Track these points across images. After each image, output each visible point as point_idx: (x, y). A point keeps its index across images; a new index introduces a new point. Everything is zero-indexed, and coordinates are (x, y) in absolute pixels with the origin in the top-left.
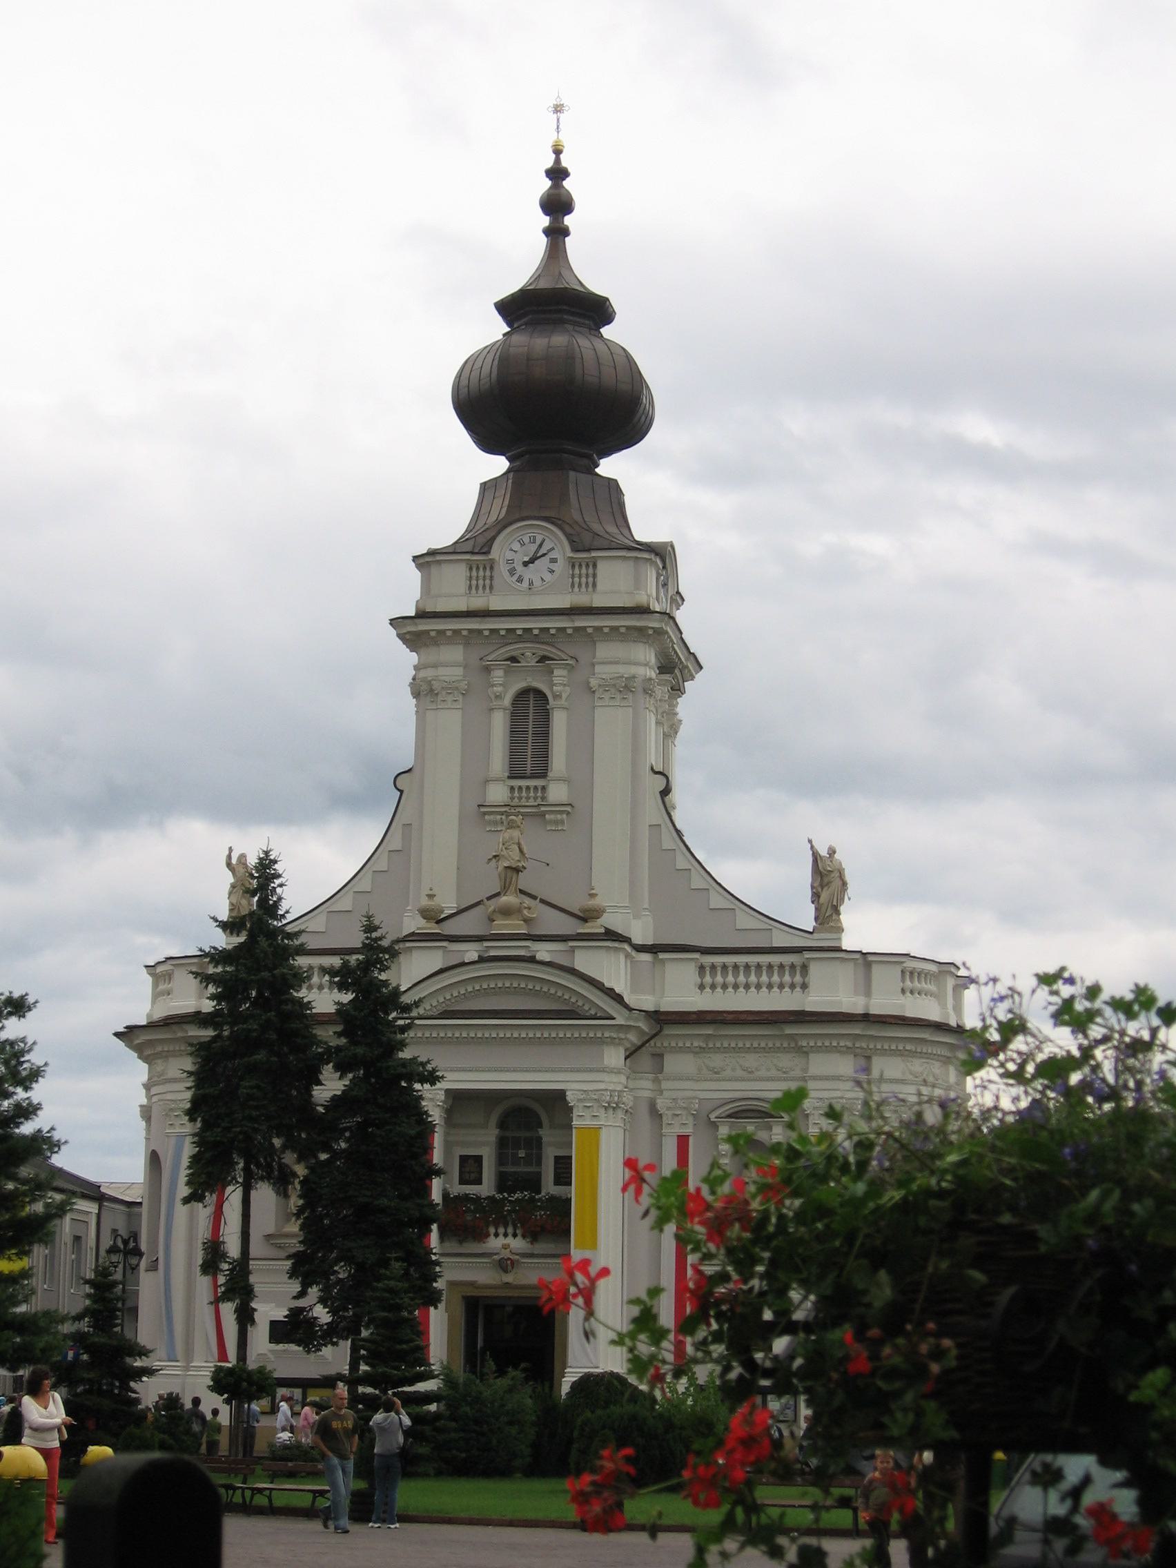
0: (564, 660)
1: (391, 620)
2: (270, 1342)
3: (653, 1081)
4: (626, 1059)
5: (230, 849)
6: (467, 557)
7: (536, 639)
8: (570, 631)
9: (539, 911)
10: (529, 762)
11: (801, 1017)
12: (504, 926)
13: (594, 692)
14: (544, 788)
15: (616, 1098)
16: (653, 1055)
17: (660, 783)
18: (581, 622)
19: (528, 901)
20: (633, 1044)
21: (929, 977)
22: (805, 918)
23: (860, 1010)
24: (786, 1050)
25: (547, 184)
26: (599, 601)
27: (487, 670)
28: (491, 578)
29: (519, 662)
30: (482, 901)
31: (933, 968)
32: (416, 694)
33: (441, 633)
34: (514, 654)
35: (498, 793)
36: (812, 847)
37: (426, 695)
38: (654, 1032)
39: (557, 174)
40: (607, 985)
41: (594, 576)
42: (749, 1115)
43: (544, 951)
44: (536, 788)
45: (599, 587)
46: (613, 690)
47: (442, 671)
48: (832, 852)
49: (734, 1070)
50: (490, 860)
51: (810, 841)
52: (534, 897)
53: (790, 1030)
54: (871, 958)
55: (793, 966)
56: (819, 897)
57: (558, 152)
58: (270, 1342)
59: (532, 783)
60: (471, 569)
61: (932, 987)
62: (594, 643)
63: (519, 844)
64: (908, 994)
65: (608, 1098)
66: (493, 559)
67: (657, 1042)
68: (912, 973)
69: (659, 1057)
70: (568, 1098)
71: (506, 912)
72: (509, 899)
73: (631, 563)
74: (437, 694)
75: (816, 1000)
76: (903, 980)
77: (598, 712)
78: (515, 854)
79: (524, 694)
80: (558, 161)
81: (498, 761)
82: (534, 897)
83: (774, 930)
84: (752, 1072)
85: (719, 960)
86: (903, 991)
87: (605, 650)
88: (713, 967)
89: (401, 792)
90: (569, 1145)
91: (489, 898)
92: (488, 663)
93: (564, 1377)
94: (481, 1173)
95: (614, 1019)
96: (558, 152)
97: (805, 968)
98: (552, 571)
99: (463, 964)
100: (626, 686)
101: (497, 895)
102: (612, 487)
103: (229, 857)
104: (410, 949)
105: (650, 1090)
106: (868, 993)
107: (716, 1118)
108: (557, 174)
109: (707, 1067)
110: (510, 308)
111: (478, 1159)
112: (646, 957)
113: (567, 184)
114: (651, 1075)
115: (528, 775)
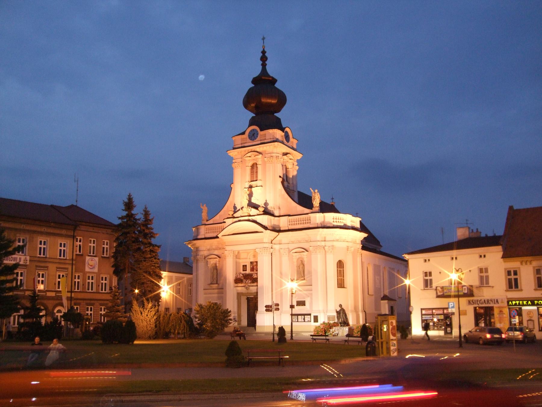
23: (317, 227)
25: (261, 54)
39: (264, 52)
80: (264, 49)
94: (246, 268)
108: (264, 52)
111: (246, 266)
115: (255, 180)
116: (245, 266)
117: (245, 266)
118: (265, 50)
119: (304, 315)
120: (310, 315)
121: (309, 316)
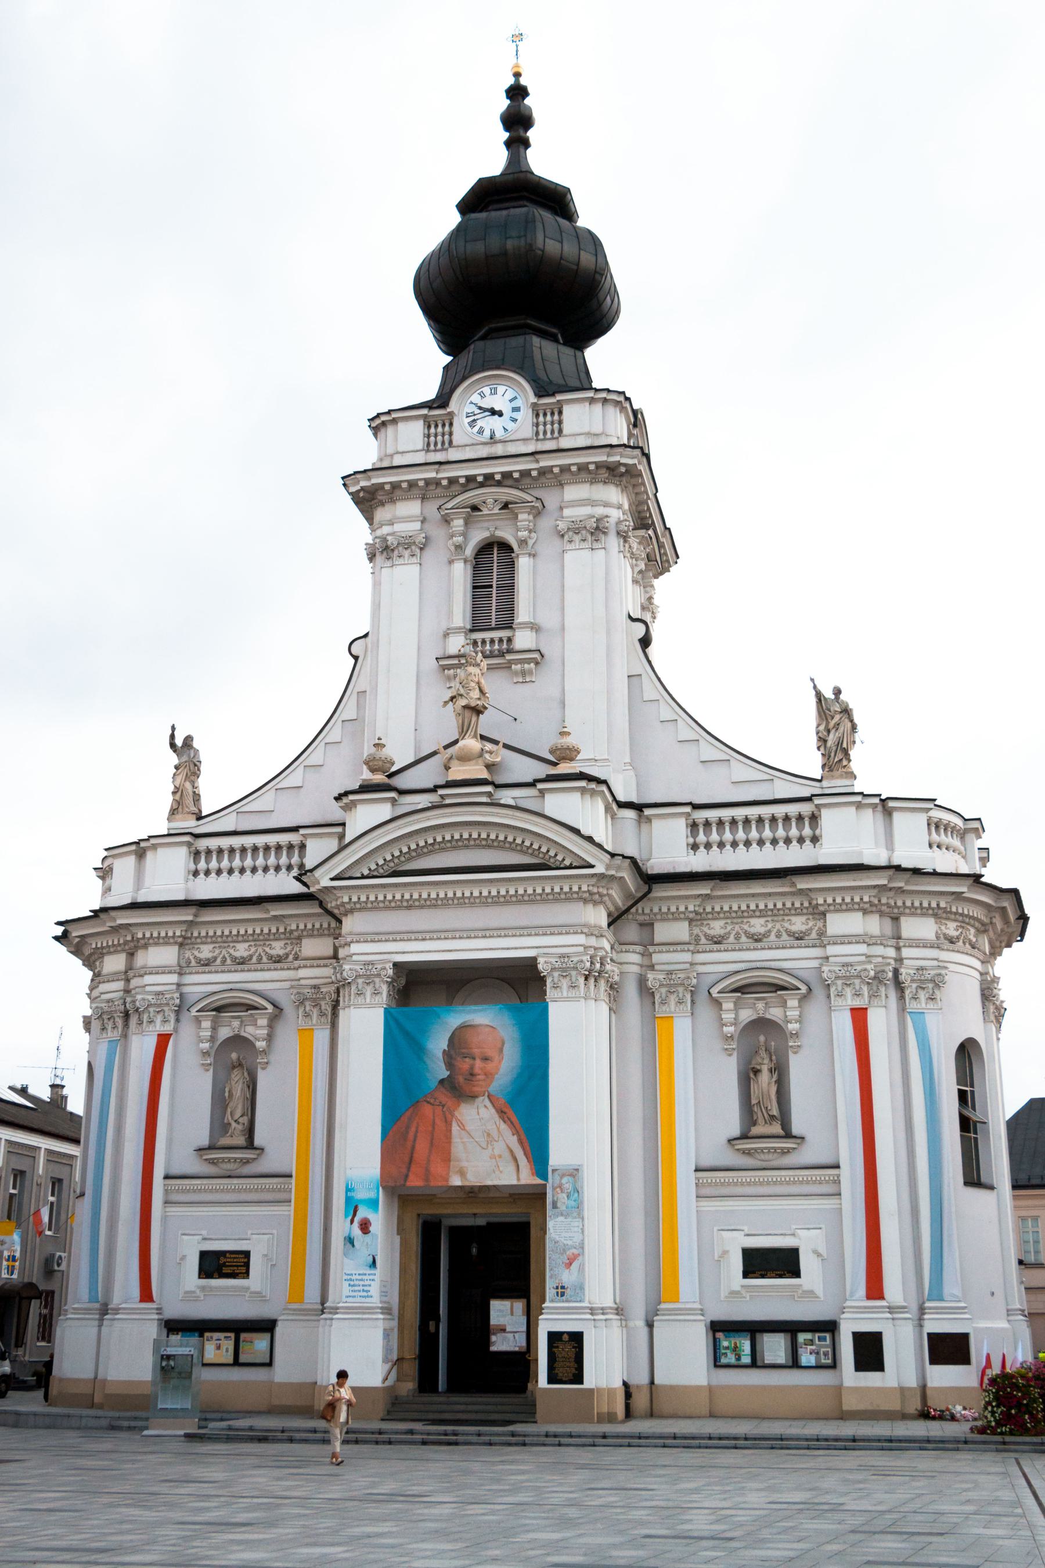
0: (528, 502)
1: (343, 478)
2: (200, 1277)
3: (643, 955)
4: (609, 925)
5: (173, 728)
6: (425, 411)
7: (499, 484)
8: (534, 473)
9: (501, 755)
10: (494, 617)
13: (563, 536)
14: (510, 640)
15: (598, 966)
16: (641, 925)
17: (640, 630)
18: (545, 462)
19: (489, 746)
20: (617, 908)
22: (812, 764)
24: (799, 912)
26: (565, 443)
27: (447, 520)
29: (481, 511)
31: (959, 822)
32: (372, 557)
33: (396, 486)
34: (476, 501)
36: (815, 687)
37: (382, 552)
38: (639, 895)
39: (517, 92)
40: (585, 832)
41: (560, 422)
42: (759, 989)
43: (507, 796)
45: (566, 430)
46: (584, 532)
47: (398, 527)
48: (837, 692)
49: (737, 937)
51: (812, 680)
53: (803, 883)
54: (891, 804)
55: (800, 818)
56: (825, 741)
57: (517, 75)
58: (200, 1277)
59: (496, 635)
61: (956, 842)
62: (562, 485)
63: (478, 683)
64: (935, 847)
65: (588, 964)
67: (644, 907)
68: (937, 827)
69: (648, 926)
70: (540, 967)
71: (465, 758)
73: (598, 407)
74: (393, 550)
75: (827, 853)
76: (930, 834)
77: (568, 556)
78: (476, 694)
79: (486, 548)
81: (460, 614)
84: (756, 941)
85: (712, 814)
86: (930, 846)
87: (573, 492)
88: (707, 824)
89: (356, 658)
92: (447, 511)
93: (542, 1314)
95: (592, 866)
96: (517, 75)
97: (814, 818)
98: (514, 420)
100: (597, 528)
101: (456, 742)
103: (172, 737)
105: (638, 964)
106: (890, 845)
107: (718, 992)
108: (517, 92)
109: (706, 936)
112: (630, 814)
113: (527, 101)
114: (639, 948)
115: (493, 626)
119: (791, 1329)
120: (830, 1327)
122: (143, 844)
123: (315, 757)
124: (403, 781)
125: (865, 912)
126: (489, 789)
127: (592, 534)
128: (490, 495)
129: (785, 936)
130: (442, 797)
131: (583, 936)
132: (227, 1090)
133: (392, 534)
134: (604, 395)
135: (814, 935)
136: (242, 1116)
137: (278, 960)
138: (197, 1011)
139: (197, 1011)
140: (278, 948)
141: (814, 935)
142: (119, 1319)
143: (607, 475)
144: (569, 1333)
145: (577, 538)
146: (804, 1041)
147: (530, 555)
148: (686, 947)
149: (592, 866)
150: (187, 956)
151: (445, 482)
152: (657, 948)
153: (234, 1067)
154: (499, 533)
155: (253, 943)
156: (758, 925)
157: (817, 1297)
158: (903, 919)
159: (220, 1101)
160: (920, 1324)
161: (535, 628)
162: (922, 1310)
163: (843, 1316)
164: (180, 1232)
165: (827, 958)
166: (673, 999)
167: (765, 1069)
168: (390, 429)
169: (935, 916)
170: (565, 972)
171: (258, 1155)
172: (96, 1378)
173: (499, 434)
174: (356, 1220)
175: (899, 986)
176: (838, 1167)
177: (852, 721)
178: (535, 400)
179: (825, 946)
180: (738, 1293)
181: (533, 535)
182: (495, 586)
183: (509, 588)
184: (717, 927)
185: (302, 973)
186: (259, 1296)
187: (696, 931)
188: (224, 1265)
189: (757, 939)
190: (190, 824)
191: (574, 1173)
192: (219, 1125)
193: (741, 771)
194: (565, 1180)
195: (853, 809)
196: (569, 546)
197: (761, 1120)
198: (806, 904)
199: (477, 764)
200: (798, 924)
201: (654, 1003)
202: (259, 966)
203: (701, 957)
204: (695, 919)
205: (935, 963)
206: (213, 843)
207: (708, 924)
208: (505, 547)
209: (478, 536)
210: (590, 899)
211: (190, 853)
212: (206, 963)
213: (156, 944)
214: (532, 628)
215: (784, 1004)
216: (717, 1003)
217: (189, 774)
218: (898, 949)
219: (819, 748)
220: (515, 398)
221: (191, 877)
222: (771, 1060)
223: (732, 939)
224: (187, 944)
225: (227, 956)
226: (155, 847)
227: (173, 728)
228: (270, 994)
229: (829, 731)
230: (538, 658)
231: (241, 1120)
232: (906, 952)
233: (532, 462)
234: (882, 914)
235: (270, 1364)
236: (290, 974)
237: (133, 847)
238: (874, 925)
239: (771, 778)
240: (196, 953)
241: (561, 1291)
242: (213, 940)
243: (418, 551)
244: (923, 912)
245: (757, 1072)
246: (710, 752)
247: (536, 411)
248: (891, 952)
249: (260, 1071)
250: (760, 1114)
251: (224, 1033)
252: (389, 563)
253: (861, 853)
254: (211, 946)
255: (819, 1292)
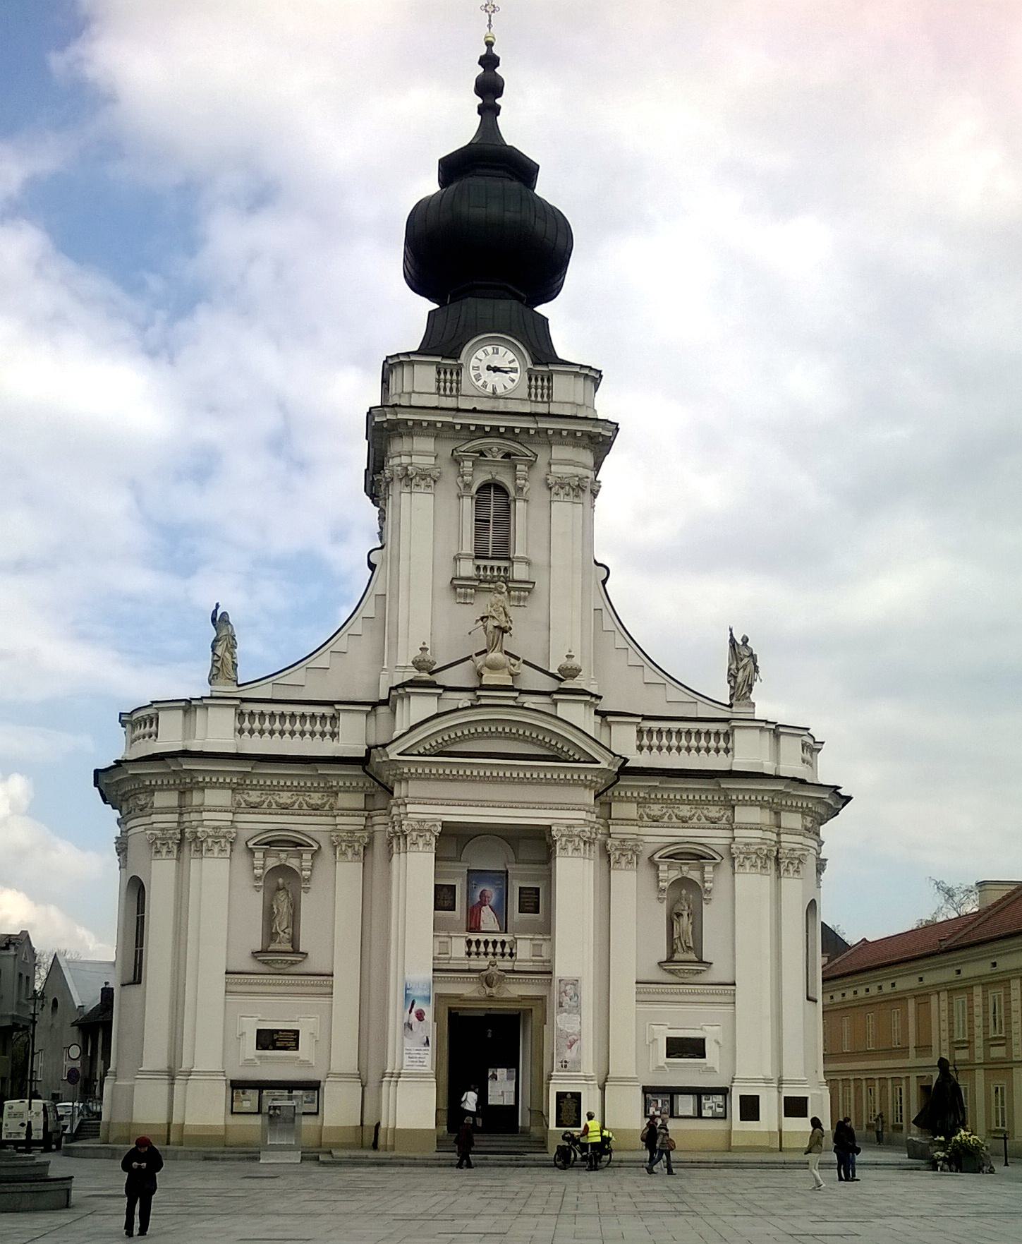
0: (527, 456)
5: (217, 605)
7: (501, 436)
11: (731, 774)
12: (490, 678)
13: (550, 489)
14: (506, 569)
19: (513, 661)
21: (805, 748)
25: (481, 70)
26: (555, 409)
28: (458, 382)
29: (486, 457)
30: (471, 656)
33: (418, 423)
34: (482, 448)
35: (467, 568)
36: (731, 635)
39: (490, 61)
42: (683, 857)
43: (529, 701)
44: (499, 568)
47: (415, 459)
48: (745, 640)
49: (670, 817)
50: (477, 621)
51: (731, 630)
52: (518, 659)
54: (781, 730)
55: (717, 734)
56: (735, 677)
57: (489, 44)
58: (257, 1049)
59: (496, 563)
60: (439, 373)
66: (462, 364)
71: (493, 667)
72: (495, 656)
74: (411, 479)
75: (740, 761)
78: (503, 617)
79: (485, 487)
82: (518, 659)
83: (699, 703)
84: (686, 822)
87: (559, 452)
88: (650, 731)
90: (549, 878)
91: (477, 655)
92: (460, 453)
95: (599, 763)
96: (489, 44)
97: (727, 736)
98: (513, 381)
99: (458, 710)
101: (485, 651)
102: (544, 321)
103: (215, 612)
104: (408, 695)
108: (490, 61)
109: (648, 816)
110: (452, 168)
112: (598, 719)
115: (490, 555)
116: (445, 890)
117: (445, 890)
118: (495, 50)
119: (699, 1093)
120: (724, 1092)
121: (719, 1099)
122: (194, 703)
123: (341, 644)
124: (443, 679)
125: (762, 807)
126: (516, 694)
127: (573, 490)
128: (496, 446)
129: (703, 820)
130: (479, 698)
131: (585, 812)
132: (275, 907)
133: (411, 464)
134: (586, 371)
135: (724, 821)
136: (286, 928)
137: (316, 808)
138: (254, 844)
139: (254, 844)
140: (316, 798)
141: (724, 821)
142: (191, 1079)
143: (587, 442)
144: (571, 1093)
145: (562, 492)
146: (714, 895)
147: (525, 500)
148: (635, 823)
149: (599, 763)
150: (237, 798)
151: (458, 427)
152: (614, 822)
153: (279, 889)
154: (498, 478)
155: (295, 793)
156: (685, 811)
157: (716, 1072)
158: (782, 813)
159: (269, 915)
160: (779, 1092)
161: (528, 563)
162: (780, 1082)
163: (734, 1084)
164: (239, 1015)
165: (734, 838)
166: (623, 860)
167: (685, 913)
168: (407, 369)
169: (803, 813)
170: (570, 839)
171: (304, 958)
172: (169, 1124)
173: (500, 391)
174: (413, 1010)
175: (777, 861)
176: (734, 984)
177: (755, 664)
178: (532, 367)
179: (733, 829)
180: (663, 1067)
181: (527, 483)
182: (491, 521)
183: (505, 525)
184: (656, 810)
185: (339, 820)
186: (306, 1064)
187: (641, 810)
188: (277, 1040)
189: (684, 820)
190: (230, 689)
191: (575, 983)
192: (270, 935)
193: (675, 694)
194: (568, 987)
195: (758, 731)
196: (556, 498)
197: (680, 949)
198: (722, 799)
199: (503, 673)
200: (714, 812)
201: (610, 861)
202: (301, 812)
203: (644, 831)
204: (642, 803)
205: (800, 846)
206: (257, 708)
207: (650, 807)
208: (500, 488)
209: (481, 478)
210: (587, 785)
211: (236, 714)
212: (254, 806)
213: (213, 788)
214: (526, 563)
215: (702, 869)
216: (655, 866)
217: (229, 646)
218: (778, 834)
219: (729, 682)
220: (514, 360)
221: (237, 734)
222: (689, 907)
223: (666, 819)
224: (238, 789)
225: (272, 801)
226: (206, 707)
227: (217, 605)
228: (312, 834)
229: (738, 670)
230: (528, 588)
231: (286, 931)
232: (783, 838)
233: (529, 421)
234: (771, 809)
235: (317, 1114)
236: (329, 820)
237: (183, 704)
238: (764, 817)
239: (695, 701)
240: (246, 797)
241: (565, 1065)
242: (262, 788)
243: (432, 482)
244: (795, 810)
245: (679, 915)
246: (651, 676)
247: (531, 375)
248: (774, 837)
249: (303, 894)
250: (679, 945)
251: (272, 862)
252: (407, 490)
253: (762, 764)
254: (258, 793)
255: (717, 1069)
